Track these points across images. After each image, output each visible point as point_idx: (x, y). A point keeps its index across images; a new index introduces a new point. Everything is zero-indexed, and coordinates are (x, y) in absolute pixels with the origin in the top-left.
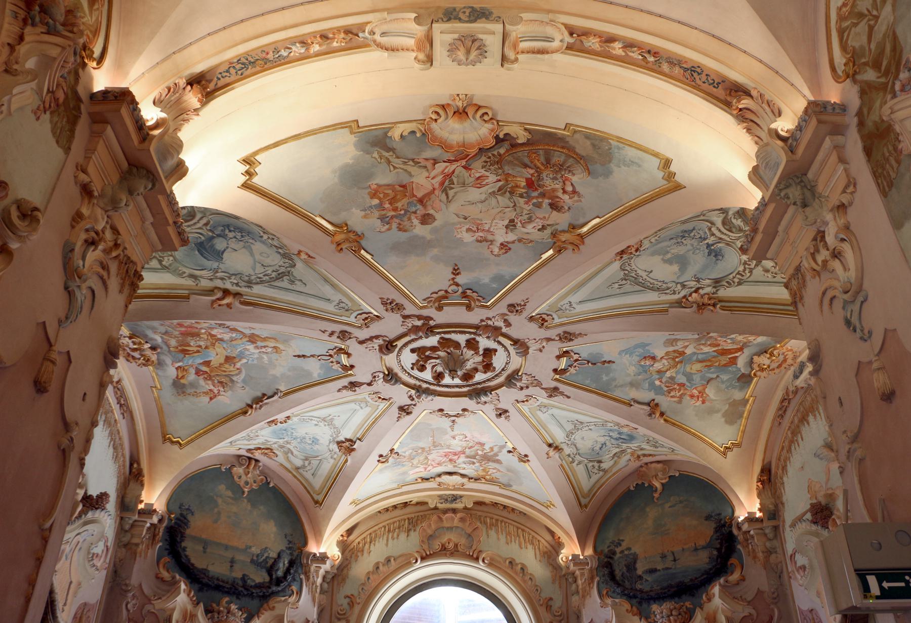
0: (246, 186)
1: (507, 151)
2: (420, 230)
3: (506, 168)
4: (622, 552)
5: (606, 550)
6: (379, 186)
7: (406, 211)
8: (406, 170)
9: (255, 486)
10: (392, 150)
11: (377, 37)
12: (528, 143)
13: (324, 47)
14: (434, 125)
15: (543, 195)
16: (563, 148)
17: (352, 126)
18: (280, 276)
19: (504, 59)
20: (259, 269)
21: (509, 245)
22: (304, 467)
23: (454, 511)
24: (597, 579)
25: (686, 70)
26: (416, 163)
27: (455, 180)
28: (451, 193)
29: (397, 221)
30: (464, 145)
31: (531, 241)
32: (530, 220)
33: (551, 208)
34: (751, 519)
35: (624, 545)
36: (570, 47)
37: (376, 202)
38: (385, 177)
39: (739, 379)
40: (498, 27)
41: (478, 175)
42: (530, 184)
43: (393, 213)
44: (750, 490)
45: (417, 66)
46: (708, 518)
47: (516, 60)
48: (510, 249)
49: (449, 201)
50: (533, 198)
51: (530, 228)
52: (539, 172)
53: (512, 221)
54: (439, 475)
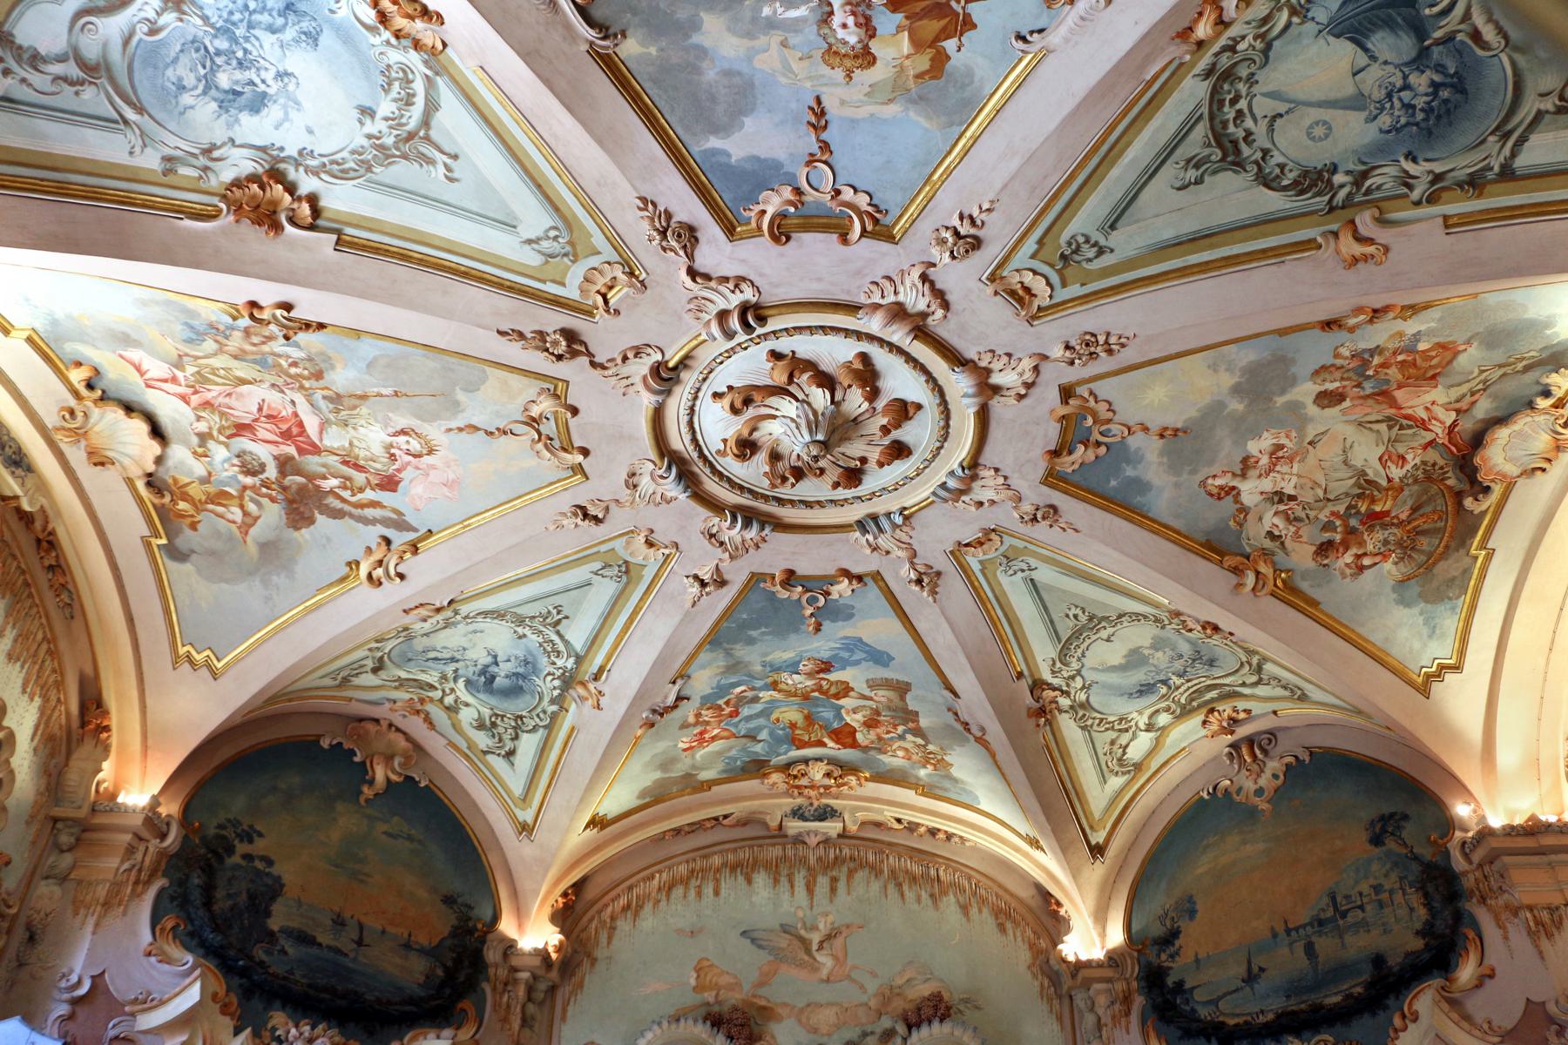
1: (1450, 488)
3: (1416, 488)
4: (248, 857)
5: (212, 831)
15: (1351, 532)
16: (1447, 547)
18: (1219, 136)
24: (160, 883)
35: (260, 846)
46: (449, 900)
52: (1401, 524)
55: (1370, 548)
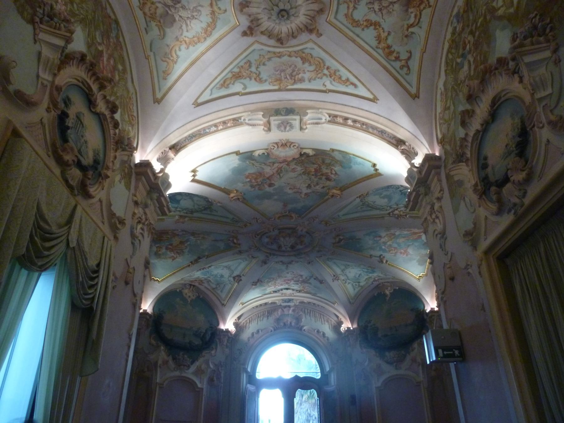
0: (193, 181)
2: (268, 189)
6: (249, 174)
7: (262, 183)
9: (194, 298)
10: (255, 160)
11: (247, 121)
12: (315, 155)
13: (224, 127)
14: (273, 151)
15: (322, 175)
17: (237, 153)
19: (301, 129)
20: (196, 207)
22: (217, 288)
23: (289, 307)
25: (379, 131)
26: (265, 164)
28: (281, 175)
30: (286, 157)
32: (317, 184)
34: (432, 311)
36: (329, 121)
37: (249, 180)
38: (252, 170)
39: (423, 245)
40: (298, 118)
42: (316, 170)
44: (432, 297)
45: (264, 132)
46: (412, 310)
47: (307, 128)
49: (281, 178)
51: (317, 187)
53: (309, 185)
54: (282, 290)
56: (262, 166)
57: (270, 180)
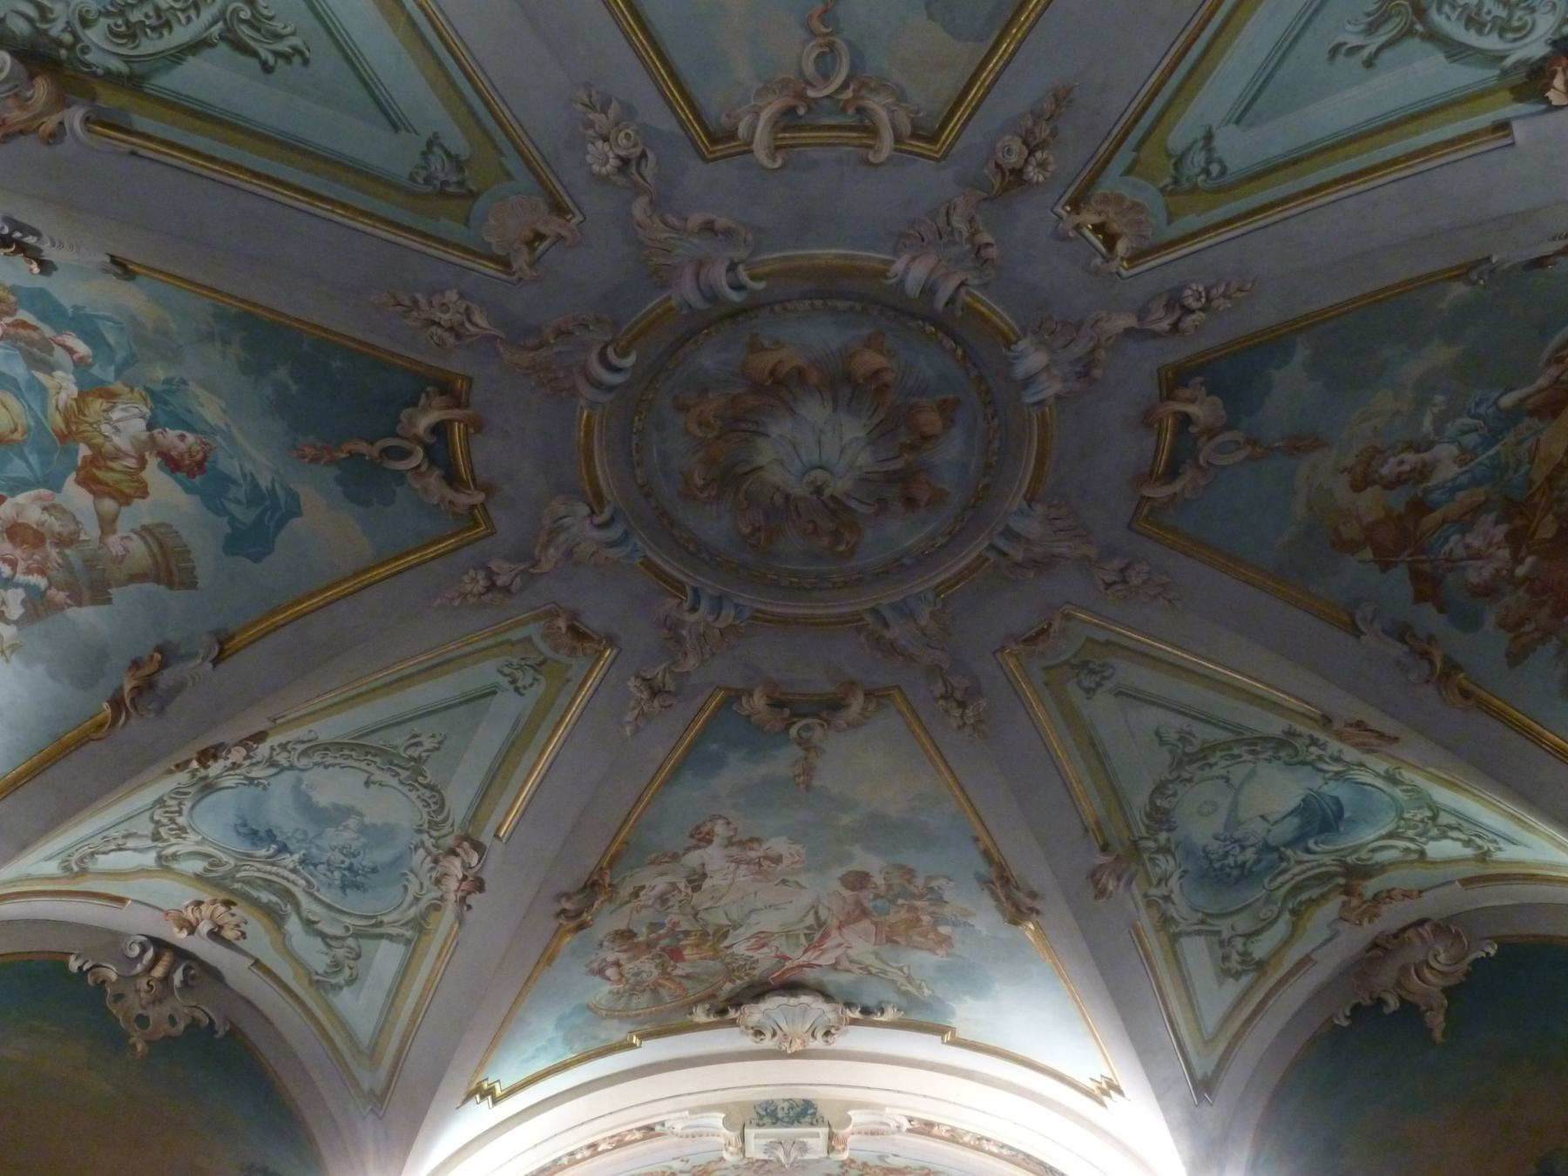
8: (883, 962)
15: (650, 945)
21: (694, 842)
27: (803, 940)
28: (810, 920)
29: (912, 888)
31: (652, 863)
32: (663, 899)
33: (630, 931)
41: (765, 950)
43: (919, 903)
48: (692, 836)
49: (814, 909)
50: (666, 936)
51: (661, 885)
53: (697, 889)
55: (629, 967)
56: (878, 964)
57: (858, 903)
